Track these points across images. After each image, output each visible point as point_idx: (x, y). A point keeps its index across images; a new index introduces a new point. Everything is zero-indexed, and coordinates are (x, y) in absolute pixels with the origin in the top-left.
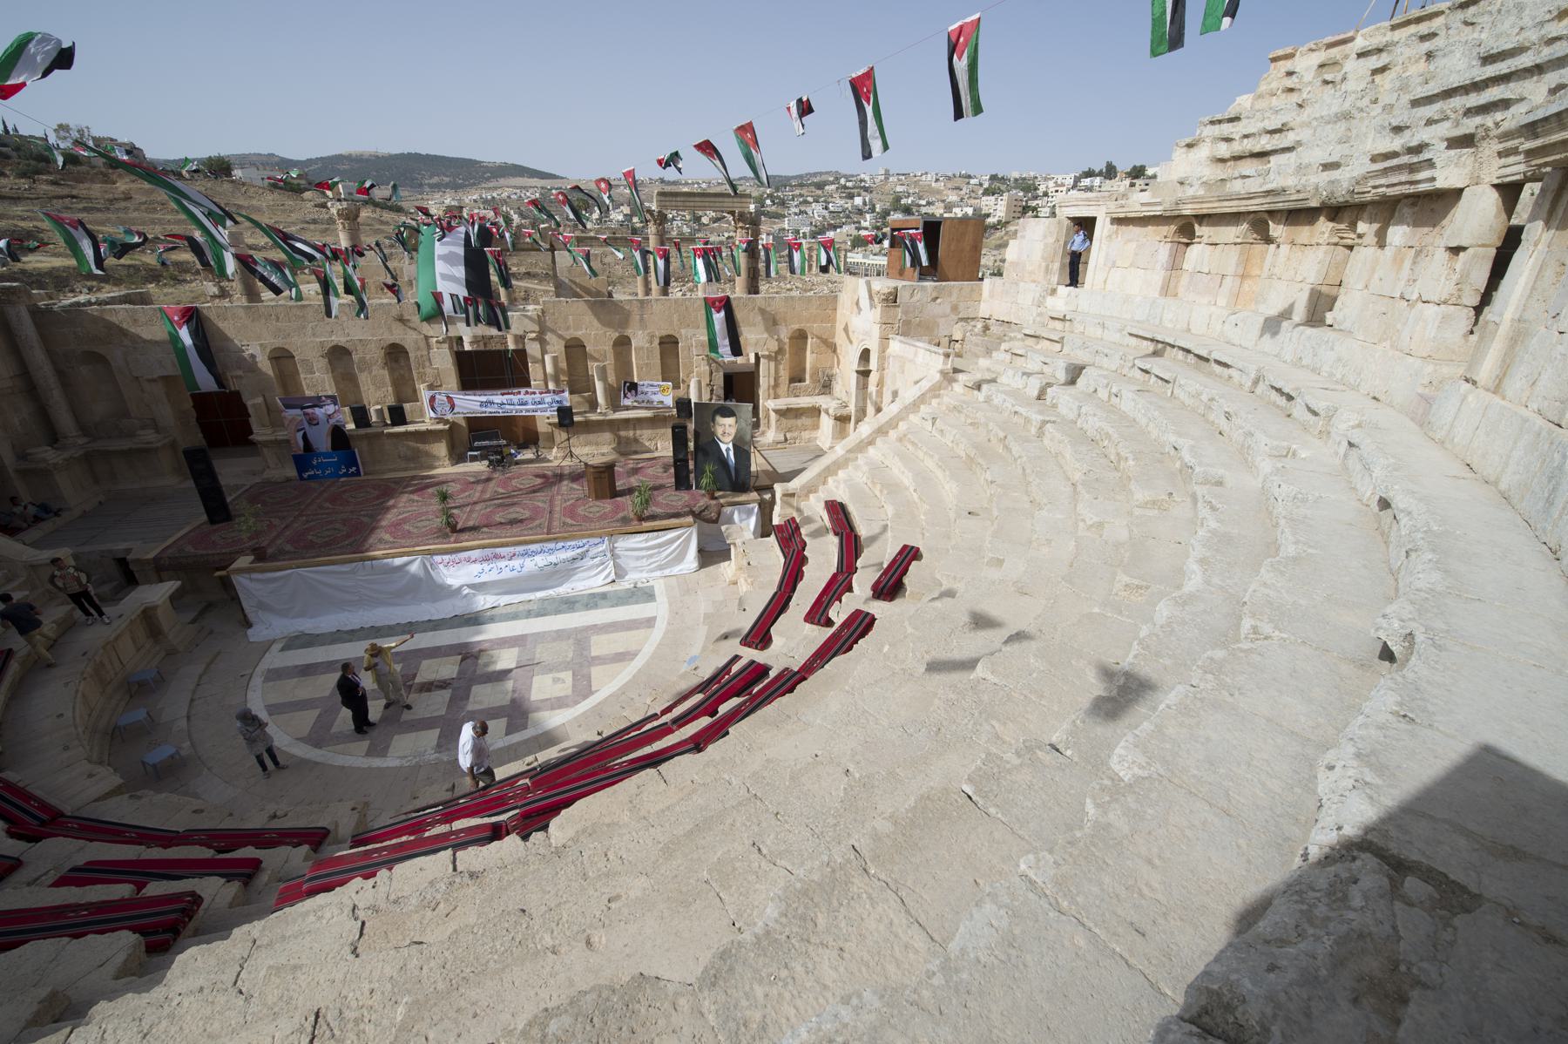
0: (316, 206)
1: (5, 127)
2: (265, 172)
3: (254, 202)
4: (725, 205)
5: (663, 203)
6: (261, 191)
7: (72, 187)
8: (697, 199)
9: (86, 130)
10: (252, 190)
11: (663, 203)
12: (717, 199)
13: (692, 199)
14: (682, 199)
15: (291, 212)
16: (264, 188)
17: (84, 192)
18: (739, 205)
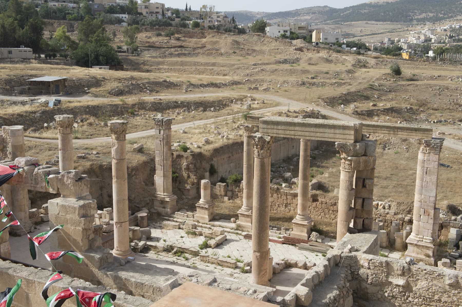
0: (296, 49)
1: (187, 7)
2: (281, 28)
3: (264, 48)
4: (326, 135)
5: (265, 130)
6: (271, 40)
7: (184, 41)
8: (297, 128)
9: (213, 7)
10: (267, 39)
11: (265, 130)
12: (317, 130)
13: (292, 128)
14: (283, 127)
15: (280, 53)
16: (273, 39)
17: (187, 44)
18: (342, 136)
